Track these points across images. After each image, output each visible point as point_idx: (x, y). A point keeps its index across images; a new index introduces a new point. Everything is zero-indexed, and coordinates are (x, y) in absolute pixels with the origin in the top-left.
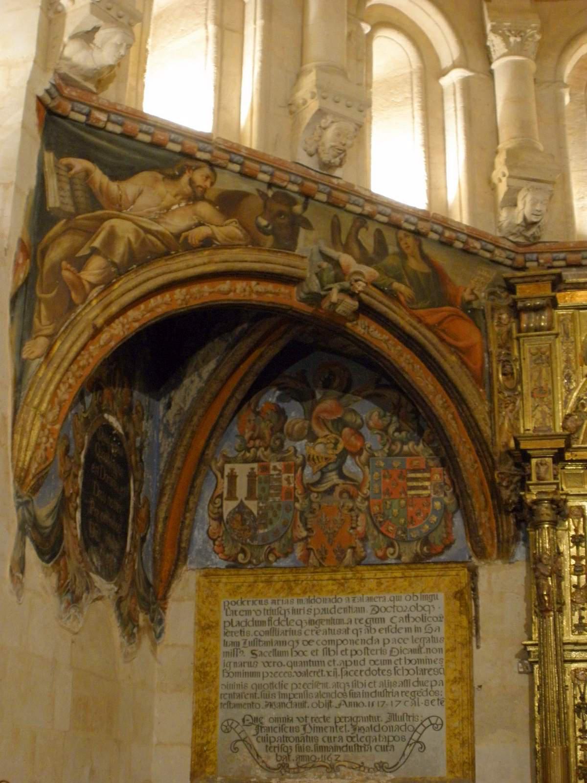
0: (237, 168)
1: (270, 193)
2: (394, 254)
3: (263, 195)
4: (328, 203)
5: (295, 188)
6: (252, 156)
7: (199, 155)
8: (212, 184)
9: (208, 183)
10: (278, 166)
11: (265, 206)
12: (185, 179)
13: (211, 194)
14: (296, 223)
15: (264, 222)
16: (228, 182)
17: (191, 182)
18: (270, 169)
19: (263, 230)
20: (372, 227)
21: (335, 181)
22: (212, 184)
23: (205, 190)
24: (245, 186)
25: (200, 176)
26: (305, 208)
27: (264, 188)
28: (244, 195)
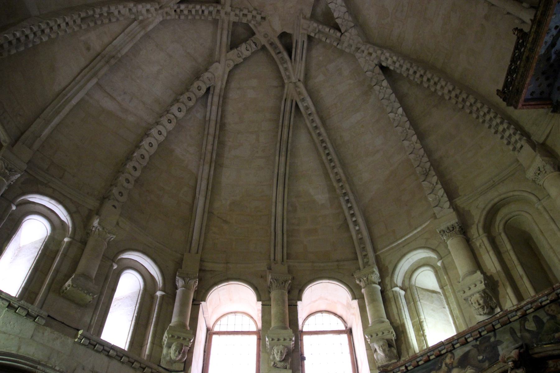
0: (458, 345)
1: (478, 343)
2: (548, 320)
3: (475, 346)
4: (502, 326)
5: (485, 332)
6: (459, 336)
7: (443, 352)
8: (454, 359)
9: (452, 360)
10: (470, 331)
11: (478, 350)
12: (444, 365)
13: (455, 364)
14: (494, 348)
15: (480, 357)
16: (459, 352)
17: (446, 364)
18: (469, 335)
19: (482, 361)
20: (530, 318)
21: (498, 315)
22: (454, 359)
23: (452, 364)
24: (466, 349)
25: (448, 361)
26: (495, 335)
27: (474, 343)
28: (468, 352)
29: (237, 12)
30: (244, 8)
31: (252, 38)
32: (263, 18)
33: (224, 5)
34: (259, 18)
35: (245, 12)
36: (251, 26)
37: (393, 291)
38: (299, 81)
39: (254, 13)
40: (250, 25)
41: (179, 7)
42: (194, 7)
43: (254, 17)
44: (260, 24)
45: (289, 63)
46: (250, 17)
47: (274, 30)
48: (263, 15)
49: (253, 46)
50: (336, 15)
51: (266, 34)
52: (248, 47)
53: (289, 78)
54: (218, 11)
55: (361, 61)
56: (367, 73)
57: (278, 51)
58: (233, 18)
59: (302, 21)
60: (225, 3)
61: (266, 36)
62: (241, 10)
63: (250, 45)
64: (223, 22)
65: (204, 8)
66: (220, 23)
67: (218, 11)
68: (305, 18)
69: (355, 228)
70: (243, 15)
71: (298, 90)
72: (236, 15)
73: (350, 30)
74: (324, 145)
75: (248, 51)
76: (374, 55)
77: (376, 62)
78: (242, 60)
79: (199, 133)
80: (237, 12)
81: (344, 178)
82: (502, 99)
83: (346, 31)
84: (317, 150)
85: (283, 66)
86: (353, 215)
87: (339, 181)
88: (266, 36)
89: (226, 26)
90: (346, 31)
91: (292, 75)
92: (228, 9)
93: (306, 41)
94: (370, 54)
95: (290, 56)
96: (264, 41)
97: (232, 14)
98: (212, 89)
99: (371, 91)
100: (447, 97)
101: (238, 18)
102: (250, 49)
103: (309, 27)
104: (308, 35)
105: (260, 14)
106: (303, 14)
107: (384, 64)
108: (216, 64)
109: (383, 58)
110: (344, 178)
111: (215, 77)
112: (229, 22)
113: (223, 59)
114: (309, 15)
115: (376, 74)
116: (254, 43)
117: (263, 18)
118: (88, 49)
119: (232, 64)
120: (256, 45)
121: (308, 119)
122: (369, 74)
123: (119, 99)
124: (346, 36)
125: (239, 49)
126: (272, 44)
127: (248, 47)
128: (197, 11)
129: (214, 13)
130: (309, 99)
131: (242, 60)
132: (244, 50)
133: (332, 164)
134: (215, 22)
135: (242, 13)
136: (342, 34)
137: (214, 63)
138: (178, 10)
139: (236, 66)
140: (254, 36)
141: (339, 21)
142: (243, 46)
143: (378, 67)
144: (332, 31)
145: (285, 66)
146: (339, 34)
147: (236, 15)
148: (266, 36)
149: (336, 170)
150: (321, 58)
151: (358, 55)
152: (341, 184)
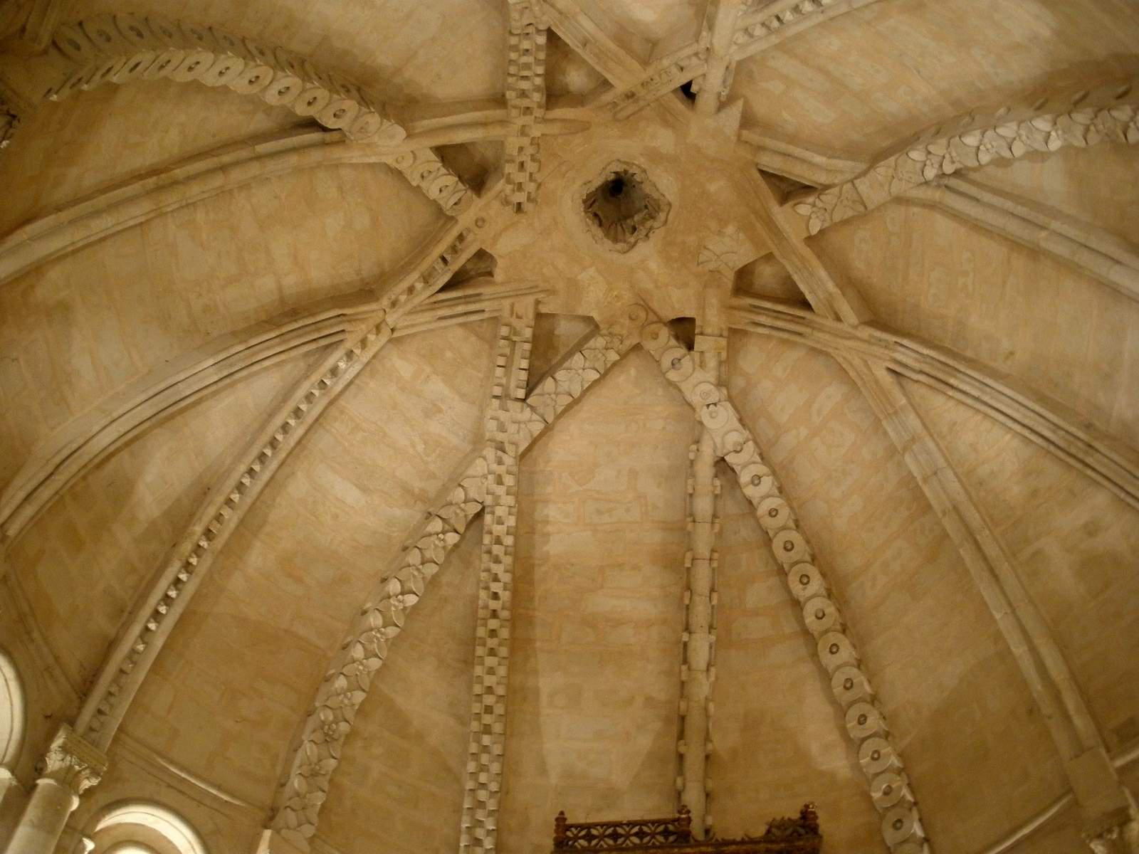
32: (519, 208)
33: (545, 121)
34: (520, 197)
35: (531, 167)
37: (81, 841)
38: (393, 330)
40: (502, 181)
41: (538, 31)
42: (538, 61)
44: (506, 202)
45: (429, 293)
47: (495, 239)
48: (528, 207)
50: (560, 375)
52: (450, 189)
53: (394, 304)
54: (527, 110)
55: (479, 467)
56: (461, 489)
57: (448, 257)
58: (513, 144)
59: (530, 300)
60: (553, 121)
61: (480, 222)
62: (533, 159)
64: (503, 122)
65: (538, 81)
66: (498, 113)
67: (527, 110)
68: (538, 302)
69: (136, 643)
70: (522, 164)
71: (372, 337)
73: (538, 418)
74: (268, 452)
75: (438, 192)
76: (501, 490)
77: (489, 500)
78: (414, 184)
79: (214, 136)
81: (219, 543)
82: (554, 835)
83: (529, 406)
84: (250, 444)
86: (156, 615)
87: (208, 534)
89: (496, 132)
90: (533, 408)
91: (401, 311)
92: (536, 132)
93: (486, 315)
94: (500, 481)
95: (444, 289)
96: (465, 220)
97: (525, 141)
98: (336, 136)
99: (416, 502)
100: (478, 689)
101: (515, 153)
102: (444, 194)
103: (519, 317)
105: (529, 199)
107: (488, 518)
108: (400, 132)
109: (500, 511)
110: (219, 543)
113: (414, 145)
115: (463, 510)
116: (460, 200)
117: (519, 208)
119: (403, 166)
120: (455, 204)
121: (313, 386)
122: (459, 495)
124: (522, 411)
126: (461, 238)
129: (525, 103)
130: (357, 367)
131: (414, 184)
133: (236, 497)
134: (499, 101)
136: (524, 400)
137: (403, 126)
138: (531, 30)
139: (399, 174)
141: (548, 384)
143: (479, 507)
144: (524, 376)
145: (419, 286)
146: (521, 393)
148: (480, 222)
149: (226, 512)
150: (449, 354)
151: (490, 453)
152: (204, 543)
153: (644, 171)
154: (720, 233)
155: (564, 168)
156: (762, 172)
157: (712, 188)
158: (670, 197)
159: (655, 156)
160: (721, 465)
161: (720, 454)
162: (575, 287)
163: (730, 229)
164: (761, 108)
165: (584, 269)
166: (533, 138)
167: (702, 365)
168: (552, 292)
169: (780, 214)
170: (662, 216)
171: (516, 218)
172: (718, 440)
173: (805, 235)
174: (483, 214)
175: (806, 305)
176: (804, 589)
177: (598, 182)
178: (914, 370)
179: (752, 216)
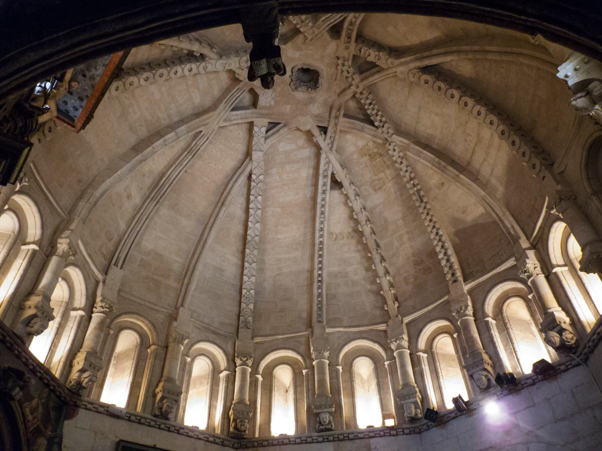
29: (350, 79)
30: (343, 76)
31: (358, 55)
32: (338, 58)
34: (340, 62)
35: (345, 74)
36: (350, 63)
39: (340, 67)
43: (343, 65)
44: (344, 57)
46: (345, 68)
47: (338, 46)
49: (363, 51)
51: (345, 48)
54: (361, 93)
58: (357, 78)
59: (310, 37)
62: (347, 78)
63: (365, 53)
70: (348, 72)
72: (353, 79)
80: (350, 79)
85: (355, 22)
88: (347, 47)
92: (353, 88)
96: (353, 45)
104: (315, 23)
105: (337, 62)
106: (305, 40)
111: (410, 70)
112: (362, 80)
114: (301, 36)
117: (338, 58)
118: (443, 184)
120: (361, 48)
123: (472, 145)
125: (374, 61)
126: (349, 37)
127: (367, 55)
128: (373, 109)
132: (372, 55)
135: (348, 75)
140: (356, 54)
142: (370, 59)
147: (353, 79)
148: (347, 48)
153: (310, 93)
154: (274, 99)
155: (334, 78)
156: (280, 123)
157: (289, 107)
158: (296, 92)
159: (311, 101)
160: (202, 57)
161: (207, 59)
162: (298, 48)
163: (272, 103)
164: (297, 133)
165: (300, 55)
166: (352, 85)
167: (239, 68)
168: (304, 43)
169: (265, 121)
170: (293, 87)
171: (336, 55)
172: (212, 61)
173: (255, 123)
174: (349, 51)
175: (233, 110)
176: (143, 78)
177: (320, 80)
178: (197, 141)
179: (271, 112)
